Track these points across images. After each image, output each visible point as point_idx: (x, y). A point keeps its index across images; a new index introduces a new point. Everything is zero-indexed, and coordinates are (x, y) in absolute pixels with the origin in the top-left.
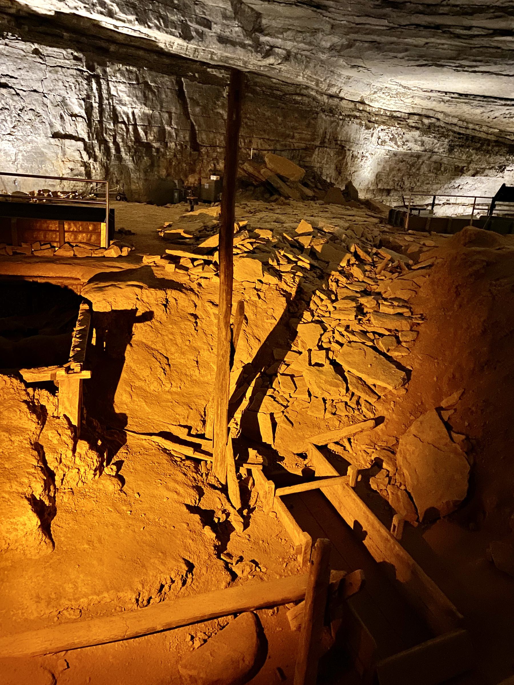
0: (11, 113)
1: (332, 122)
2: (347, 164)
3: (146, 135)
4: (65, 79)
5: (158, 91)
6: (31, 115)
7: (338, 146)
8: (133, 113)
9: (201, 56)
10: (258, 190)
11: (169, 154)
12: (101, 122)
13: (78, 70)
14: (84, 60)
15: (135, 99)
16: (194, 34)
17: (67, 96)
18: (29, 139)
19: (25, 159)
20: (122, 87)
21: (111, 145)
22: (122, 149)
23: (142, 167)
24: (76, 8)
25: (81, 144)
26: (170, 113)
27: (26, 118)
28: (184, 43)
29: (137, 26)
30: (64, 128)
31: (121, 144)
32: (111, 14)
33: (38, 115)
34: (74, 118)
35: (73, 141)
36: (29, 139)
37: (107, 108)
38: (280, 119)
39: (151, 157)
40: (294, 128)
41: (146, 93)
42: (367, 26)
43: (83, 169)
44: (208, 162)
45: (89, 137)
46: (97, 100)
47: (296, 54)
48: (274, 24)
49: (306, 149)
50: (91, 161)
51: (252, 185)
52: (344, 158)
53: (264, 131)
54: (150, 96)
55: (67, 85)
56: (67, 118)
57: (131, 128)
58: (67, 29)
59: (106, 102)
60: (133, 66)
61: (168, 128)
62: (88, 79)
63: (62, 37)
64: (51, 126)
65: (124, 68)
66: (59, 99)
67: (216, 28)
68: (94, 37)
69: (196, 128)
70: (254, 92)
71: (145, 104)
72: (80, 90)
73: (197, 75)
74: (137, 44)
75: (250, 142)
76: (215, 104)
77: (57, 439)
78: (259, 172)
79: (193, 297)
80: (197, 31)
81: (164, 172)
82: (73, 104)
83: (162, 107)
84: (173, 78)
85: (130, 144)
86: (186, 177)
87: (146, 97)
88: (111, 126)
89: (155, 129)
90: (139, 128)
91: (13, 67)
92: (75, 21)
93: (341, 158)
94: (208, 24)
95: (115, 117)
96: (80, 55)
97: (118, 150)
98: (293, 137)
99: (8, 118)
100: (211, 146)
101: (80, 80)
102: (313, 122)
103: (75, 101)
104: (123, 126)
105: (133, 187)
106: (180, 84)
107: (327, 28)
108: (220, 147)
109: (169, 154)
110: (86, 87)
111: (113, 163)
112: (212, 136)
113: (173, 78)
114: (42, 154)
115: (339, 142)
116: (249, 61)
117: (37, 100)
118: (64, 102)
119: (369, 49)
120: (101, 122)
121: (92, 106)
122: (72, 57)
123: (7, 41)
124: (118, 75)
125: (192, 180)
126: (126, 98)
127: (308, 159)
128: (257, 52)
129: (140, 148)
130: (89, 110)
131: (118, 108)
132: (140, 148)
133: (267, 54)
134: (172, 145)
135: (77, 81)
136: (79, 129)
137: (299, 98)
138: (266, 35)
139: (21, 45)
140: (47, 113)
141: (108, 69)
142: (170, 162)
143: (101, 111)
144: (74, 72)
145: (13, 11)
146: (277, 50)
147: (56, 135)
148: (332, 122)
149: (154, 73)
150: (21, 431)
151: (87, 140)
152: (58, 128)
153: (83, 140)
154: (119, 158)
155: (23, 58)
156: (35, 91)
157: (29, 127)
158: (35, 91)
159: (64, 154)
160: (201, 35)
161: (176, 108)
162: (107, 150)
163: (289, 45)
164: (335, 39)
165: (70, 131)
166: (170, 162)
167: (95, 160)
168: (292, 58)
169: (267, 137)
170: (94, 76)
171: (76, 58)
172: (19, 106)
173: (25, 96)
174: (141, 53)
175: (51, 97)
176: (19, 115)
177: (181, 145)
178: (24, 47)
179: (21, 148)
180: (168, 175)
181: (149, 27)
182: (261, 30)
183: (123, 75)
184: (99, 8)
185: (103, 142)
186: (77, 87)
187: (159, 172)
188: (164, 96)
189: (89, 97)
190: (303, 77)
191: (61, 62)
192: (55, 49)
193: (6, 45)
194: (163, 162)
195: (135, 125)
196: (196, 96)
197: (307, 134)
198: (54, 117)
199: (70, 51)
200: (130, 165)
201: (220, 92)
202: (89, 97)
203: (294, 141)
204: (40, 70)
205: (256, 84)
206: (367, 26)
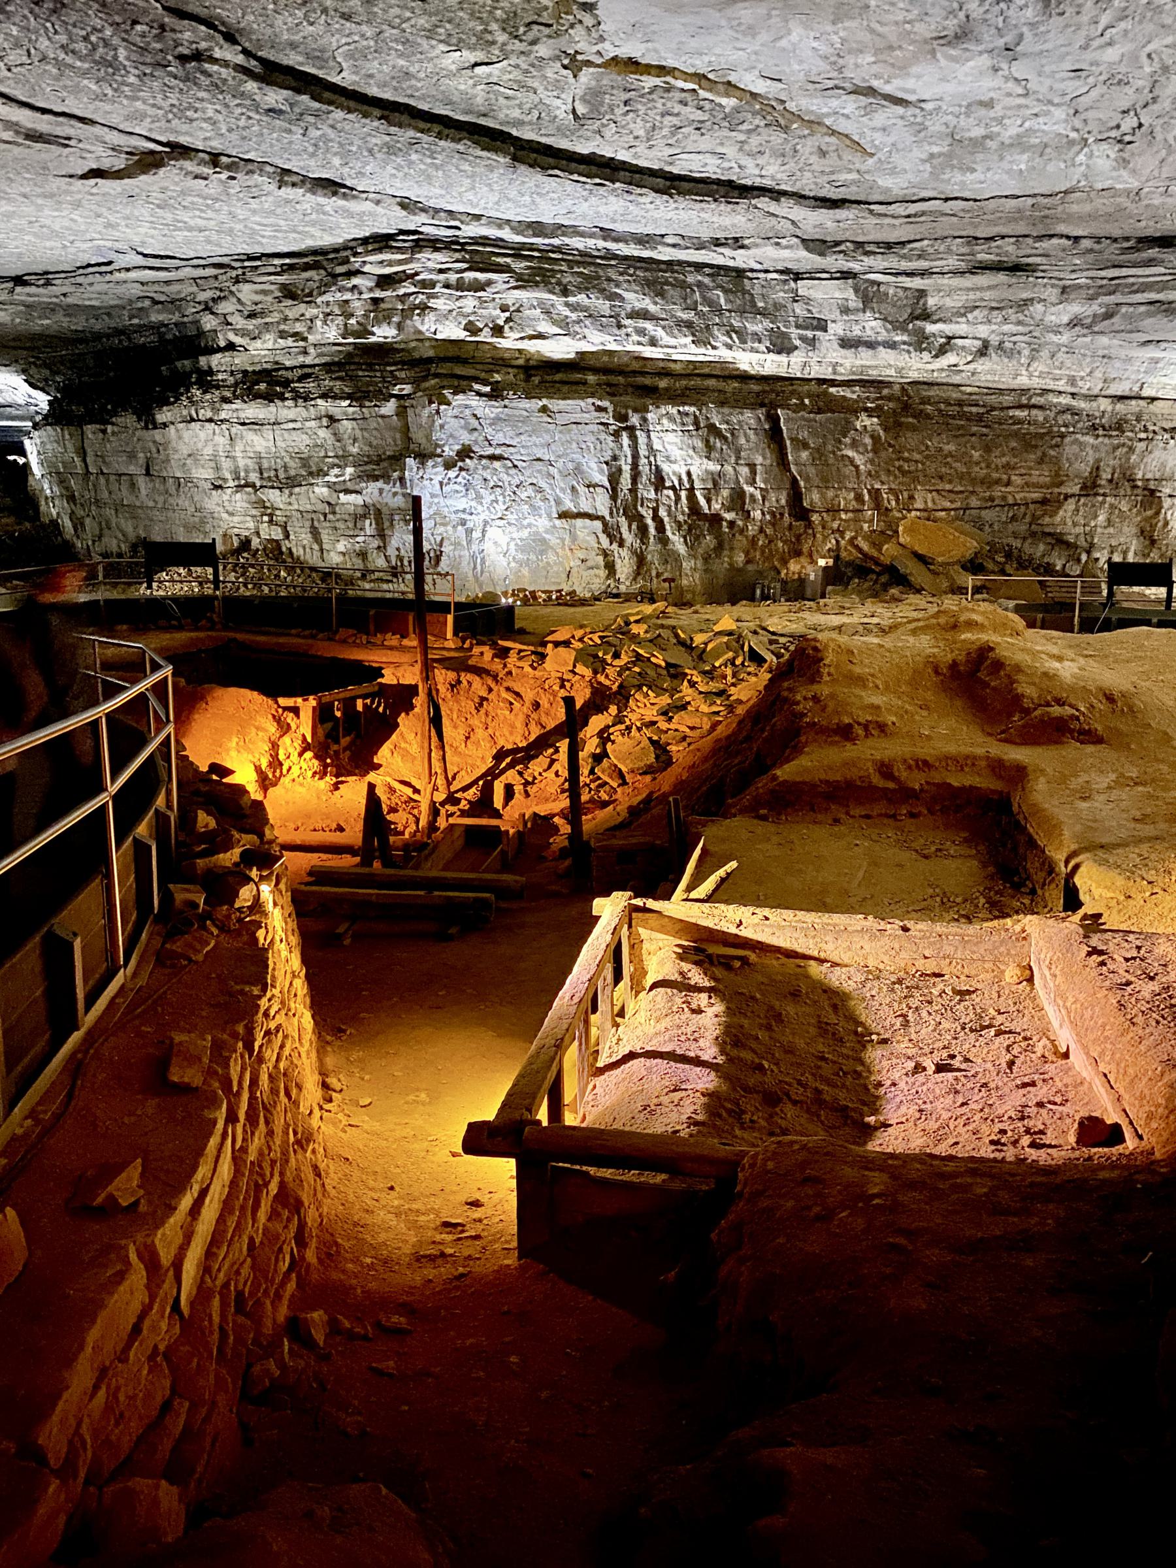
1: (1116, 448)
2: (1166, 523)
3: (709, 501)
4: (581, 438)
5: (733, 434)
6: (530, 491)
7: (1139, 491)
8: (689, 474)
9: (816, 372)
10: (883, 579)
11: (752, 530)
12: (633, 490)
14: (611, 409)
15: (691, 452)
16: (797, 342)
18: (525, 522)
19: (519, 549)
20: (670, 437)
21: (649, 521)
22: (668, 527)
23: (700, 551)
25: (598, 525)
26: (752, 467)
27: (523, 496)
28: (783, 358)
29: (693, 349)
30: (577, 505)
31: (666, 519)
32: (653, 342)
33: (540, 490)
35: (587, 521)
36: (525, 522)
37: (644, 469)
38: (976, 455)
39: (719, 536)
40: (1007, 466)
41: (711, 438)
42: (1132, 280)
43: (601, 558)
44: (825, 538)
45: (611, 513)
46: (630, 460)
47: (1001, 343)
48: (948, 302)
49: (1044, 502)
50: (615, 546)
51: (873, 571)
52: (1158, 513)
53: (941, 478)
54: (718, 445)
57: (683, 494)
58: (596, 370)
59: (643, 461)
60: (691, 405)
61: (748, 489)
62: (616, 434)
63: (585, 383)
64: (558, 502)
65: (673, 410)
66: (570, 466)
67: (836, 329)
68: (635, 373)
69: (802, 484)
70: (920, 415)
71: (708, 458)
73: (807, 401)
74: (706, 371)
75: (911, 497)
76: (840, 442)
77: (289, 746)
78: (880, 550)
79: (490, 682)
80: (803, 339)
81: (740, 558)
83: (738, 458)
84: (761, 413)
85: (681, 518)
86: (785, 562)
87: (709, 447)
88: (652, 495)
89: (725, 493)
90: (698, 493)
91: (511, 433)
92: (606, 359)
93: (1149, 513)
94: (822, 325)
95: (659, 481)
96: (605, 403)
97: (661, 528)
98: (1008, 484)
99: (500, 498)
100: (828, 511)
101: (603, 436)
102: (1052, 453)
103: (594, 466)
104: (671, 493)
105: (685, 582)
106: (774, 420)
107: (1052, 294)
108: (846, 511)
109: (752, 530)
110: (612, 445)
111: (651, 548)
112: (830, 494)
113: (761, 413)
114: (544, 541)
115: (1139, 483)
116: (915, 366)
117: (539, 471)
118: (578, 470)
119: (1149, 315)
120: (633, 490)
121: (620, 470)
123: (506, 402)
124: (665, 421)
125: (794, 566)
126: (676, 453)
127: (1047, 520)
128: (921, 351)
129: (698, 522)
131: (666, 468)
132: (698, 522)
133: (942, 351)
134: (757, 514)
136: (598, 504)
137: (1019, 413)
138: (935, 322)
139: (525, 404)
141: (649, 416)
142: (753, 541)
143: (635, 476)
144: (595, 428)
145: (521, 362)
146: (959, 342)
147: (563, 515)
148: (1116, 448)
149: (726, 410)
150: (265, 730)
151: (608, 518)
152: (569, 505)
154: (663, 540)
156: (539, 460)
158: (539, 460)
159: (574, 538)
160: (812, 343)
161: (764, 458)
162: (643, 530)
163: (983, 331)
164: (1076, 308)
165: (585, 507)
166: (753, 541)
167: (621, 545)
168: (991, 351)
169: (948, 487)
170: (624, 429)
171: (600, 409)
172: (516, 481)
174: (712, 382)
175: (559, 465)
177: (773, 514)
179: (515, 535)
180: (748, 562)
181: (714, 348)
182: (926, 316)
183: (672, 419)
184: (636, 338)
185: (634, 517)
187: (731, 558)
188: (742, 441)
189: (615, 458)
190: (1030, 376)
191: (578, 417)
194: (741, 541)
195: (691, 490)
196: (804, 434)
197: (1041, 475)
198: (563, 490)
199: (590, 400)
200: (681, 548)
201: (848, 422)
202: (615, 458)
203: (1009, 489)
204: (547, 431)
205: (926, 401)
206: (1132, 280)
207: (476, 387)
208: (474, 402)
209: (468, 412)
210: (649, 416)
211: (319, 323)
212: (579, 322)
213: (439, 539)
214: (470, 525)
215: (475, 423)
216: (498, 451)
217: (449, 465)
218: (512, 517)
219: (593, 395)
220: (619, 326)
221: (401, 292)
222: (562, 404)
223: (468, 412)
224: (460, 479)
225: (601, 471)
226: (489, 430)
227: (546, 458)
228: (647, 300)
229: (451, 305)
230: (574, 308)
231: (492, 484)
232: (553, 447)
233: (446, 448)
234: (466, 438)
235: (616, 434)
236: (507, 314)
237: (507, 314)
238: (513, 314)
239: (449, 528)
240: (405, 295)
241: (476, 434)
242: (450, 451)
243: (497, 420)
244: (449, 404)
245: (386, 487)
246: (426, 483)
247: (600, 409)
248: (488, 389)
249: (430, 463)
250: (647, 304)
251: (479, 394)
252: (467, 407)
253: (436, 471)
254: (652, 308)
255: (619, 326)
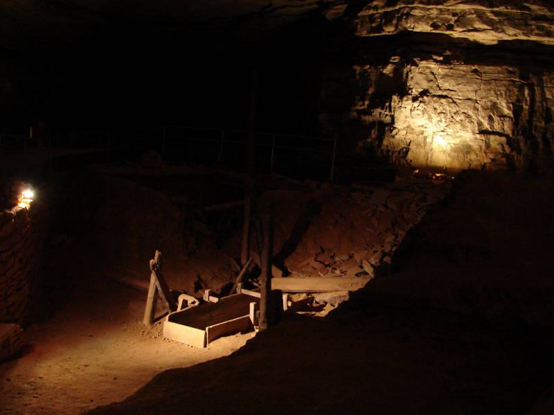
0: (447, 115)
6: (462, 117)
13: (511, 81)
17: (498, 102)
18: (458, 134)
24: (515, 35)
25: (503, 139)
30: (492, 127)
33: (468, 116)
34: (502, 119)
36: (458, 134)
45: (513, 133)
46: (528, 103)
55: (499, 93)
56: (495, 118)
62: (521, 88)
64: (480, 124)
66: (489, 104)
72: (510, 96)
82: (503, 107)
101: (511, 88)
103: (504, 104)
117: (469, 106)
118: (494, 107)
120: (530, 122)
121: (522, 108)
122: (506, 71)
123: (452, 66)
130: (517, 110)
135: (508, 90)
136: (506, 127)
139: (464, 68)
140: (477, 115)
141: (544, 78)
144: (507, 83)
145: (463, 45)
151: (511, 136)
152: (486, 125)
153: (507, 136)
155: (463, 76)
156: (469, 99)
157: (459, 125)
165: (497, 127)
170: (526, 85)
171: (510, 72)
173: (460, 103)
176: (452, 117)
178: (465, 68)
184: (536, 32)
186: (508, 94)
192: (491, 67)
193: (451, 68)
198: (483, 118)
199: (504, 67)
202: (518, 100)
204: (476, 83)
207: (435, 57)
208: (433, 66)
209: (428, 71)
210: (544, 78)
211: (359, 27)
212: (500, 22)
213: (408, 141)
214: (426, 134)
215: (431, 77)
216: (444, 93)
217: (415, 99)
218: (450, 131)
219: (506, 64)
220: (527, 25)
221: (397, 8)
222: (487, 68)
223: (428, 71)
224: (420, 107)
225: (509, 108)
226: (440, 82)
227: (474, 98)
228: (546, 10)
229: (423, 13)
230: (496, 14)
231: (439, 111)
232: (479, 92)
233: (414, 90)
234: (425, 85)
235: (521, 88)
236: (456, 18)
237: (456, 18)
238: (461, 19)
239: (415, 135)
240: (400, 9)
241: (432, 83)
242: (415, 92)
243: (445, 76)
244: (417, 65)
245: (383, 112)
246: (402, 109)
247: (510, 72)
248: (441, 58)
249: (405, 98)
250: (546, 12)
251: (436, 61)
252: (428, 68)
253: (408, 104)
254: (549, 14)
255: (527, 25)
